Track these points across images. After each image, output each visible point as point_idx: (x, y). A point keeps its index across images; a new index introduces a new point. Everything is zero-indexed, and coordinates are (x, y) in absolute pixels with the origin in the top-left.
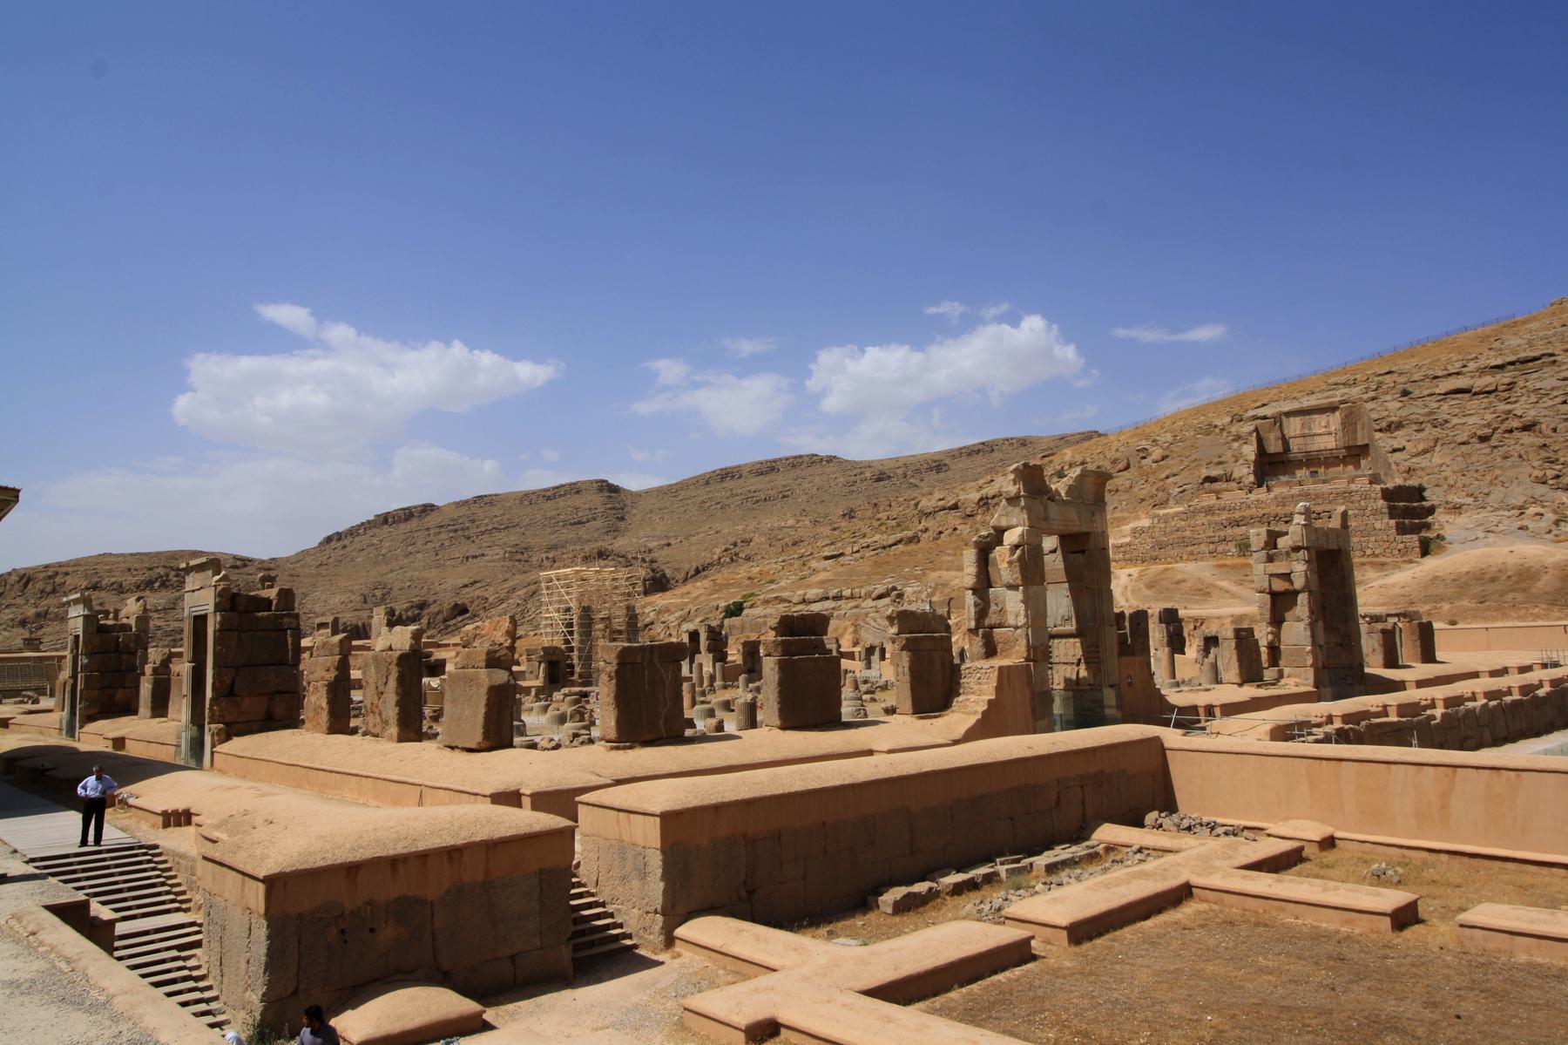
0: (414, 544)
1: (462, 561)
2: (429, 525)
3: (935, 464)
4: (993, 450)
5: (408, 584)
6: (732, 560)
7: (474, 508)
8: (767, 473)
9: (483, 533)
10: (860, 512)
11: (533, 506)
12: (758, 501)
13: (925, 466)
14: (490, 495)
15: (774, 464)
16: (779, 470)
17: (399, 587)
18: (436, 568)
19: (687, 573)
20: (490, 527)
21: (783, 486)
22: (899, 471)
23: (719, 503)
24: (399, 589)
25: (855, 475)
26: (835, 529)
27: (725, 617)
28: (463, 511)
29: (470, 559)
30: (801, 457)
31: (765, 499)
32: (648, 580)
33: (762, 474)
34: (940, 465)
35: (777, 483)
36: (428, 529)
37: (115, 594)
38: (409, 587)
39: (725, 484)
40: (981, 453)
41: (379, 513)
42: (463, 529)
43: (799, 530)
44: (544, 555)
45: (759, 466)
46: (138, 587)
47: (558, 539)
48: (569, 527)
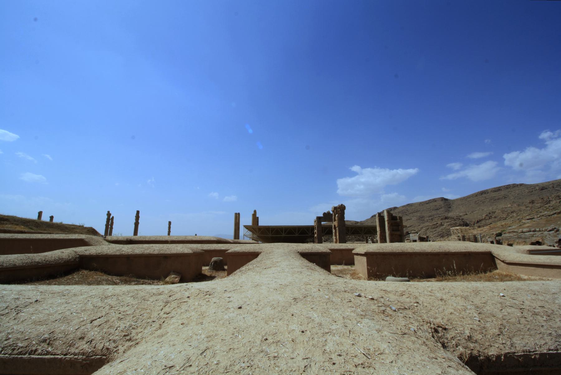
6: (490, 218)
7: (407, 207)
8: (497, 191)
9: (410, 213)
12: (495, 200)
15: (499, 188)
16: (502, 190)
19: (474, 222)
20: (412, 212)
26: (527, 207)
27: (496, 237)
28: (405, 208)
30: (509, 185)
36: (396, 213)
39: (483, 196)
42: (405, 213)
43: (513, 208)
44: (428, 219)
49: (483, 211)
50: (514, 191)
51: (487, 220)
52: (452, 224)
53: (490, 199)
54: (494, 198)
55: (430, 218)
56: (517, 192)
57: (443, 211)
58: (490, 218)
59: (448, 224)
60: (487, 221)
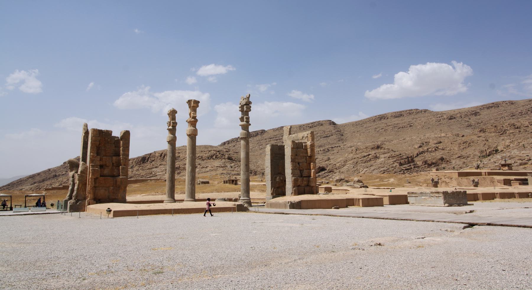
3: (474, 112)
4: (498, 106)
6: (436, 150)
8: (399, 117)
10: (488, 130)
12: (399, 128)
22: (459, 115)
25: (440, 117)
30: (412, 110)
31: (403, 127)
32: (410, 158)
34: (476, 113)
40: (493, 108)
42: (279, 139)
43: (449, 138)
44: (319, 149)
45: (395, 114)
46: (208, 158)
47: (321, 143)
51: (431, 152)
52: (395, 157)
53: (392, 126)
54: (398, 125)
56: (423, 119)
58: (436, 150)
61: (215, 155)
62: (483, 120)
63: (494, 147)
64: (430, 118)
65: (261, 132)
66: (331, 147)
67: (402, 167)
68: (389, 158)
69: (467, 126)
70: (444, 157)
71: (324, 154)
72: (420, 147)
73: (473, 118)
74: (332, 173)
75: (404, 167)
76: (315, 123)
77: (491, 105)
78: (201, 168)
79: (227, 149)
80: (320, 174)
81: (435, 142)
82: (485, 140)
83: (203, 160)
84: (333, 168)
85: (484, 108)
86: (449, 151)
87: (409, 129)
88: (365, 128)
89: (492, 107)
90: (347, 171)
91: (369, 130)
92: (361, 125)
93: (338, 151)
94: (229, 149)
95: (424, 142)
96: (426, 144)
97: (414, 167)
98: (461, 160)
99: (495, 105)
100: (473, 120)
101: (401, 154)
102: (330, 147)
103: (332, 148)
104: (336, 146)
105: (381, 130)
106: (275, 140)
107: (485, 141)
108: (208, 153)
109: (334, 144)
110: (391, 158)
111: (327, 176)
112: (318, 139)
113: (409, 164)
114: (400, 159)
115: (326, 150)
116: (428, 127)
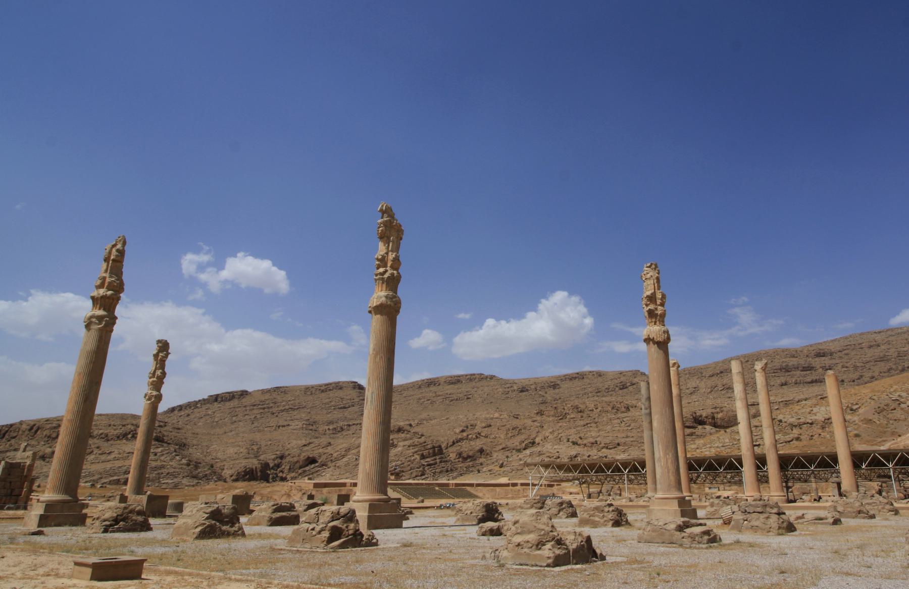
0: (237, 415)
1: (276, 428)
2: (246, 404)
3: (552, 384)
5: (270, 442)
6: (477, 437)
7: (274, 395)
9: (282, 411)
11: (313, 395)
12: (452, 400)
13: (547, 385)
14: (283, 387)
16: (462, 382)
17: (265, 444)
18: (258, 432)
19: (448, 444)
20: (287, 407)
21: (467, 392)
22: (533, 387)
23: (429, 400)
24: (265, 446)
25: (508, 388)
28: (267, 396)
29: (281, 428)
30: (474, 375)
32: (437, 447)
33: (452, 384)
34: (555, 385)
35: (463, 390)
36: (245, 406)
37: (104, 441)
38: (271, 444)
40: (577, 379)
41: (212, 394)
42: (268, 408)
43: (503, 420)
45: (450, 379)
46: (118, 437)
47: (333, 417)
48: (338, 410)
49: (448, 420)
50: (481, 388)
51: (471, 440)
52: (417, 445)
53: (443, 397)
54: (451, 396)
55: (331, 427)
56: (486, 389)
57: (356, 412)
58: (477, 437)
59: (407, 443)
60: (472, 443)
61: (132, 433)
62: (562, 395)
63: (532, 438)
64: (496, 388)
65: (239, 393)
66: (347, 425)
67: (423, 462)
68: (409, 446)
69: (541, 403)
70: (485, 448)
71: (332, 436)
72: (463, 431)
73: (551, 391)
74: (324, 467)
75: (426, 462)
76: (331, 384)
77: (574, 376)
78: (100, 454)
79: (162, 422)
80: (307, 468)
81: (484, 425)
82: (540, 426)
83: (108, 440)
84: (327, 460)
85: (566, 378)
86: (493, 440)
87: (465, 402)
88: (406, 397)
89: (575, 378)
90: (346, 466)
91: (410, 400)
92: (400, 392)
93: (354, 432)
94: (166, 423)
95: (469, 425)
96: (472, 427)
97: (441, 462)
98: (504, 453)
99: (580, 376)
100: (550, 394)
101: (425, 442)
102: (346, 424)
103: (349, 425)
104: (356, 422)
105: (427, 402)
106: (261, 408)
107: (539, 428)
108: (121, 428)
109: (353, 419)
110: (411, 448)
111: (317, 472)
112: (330, 411)
113: (434, 456)
114: (423, 449)
115: (339, 429)
116: (491, 401)
